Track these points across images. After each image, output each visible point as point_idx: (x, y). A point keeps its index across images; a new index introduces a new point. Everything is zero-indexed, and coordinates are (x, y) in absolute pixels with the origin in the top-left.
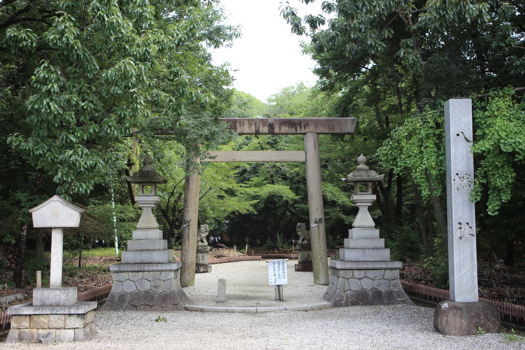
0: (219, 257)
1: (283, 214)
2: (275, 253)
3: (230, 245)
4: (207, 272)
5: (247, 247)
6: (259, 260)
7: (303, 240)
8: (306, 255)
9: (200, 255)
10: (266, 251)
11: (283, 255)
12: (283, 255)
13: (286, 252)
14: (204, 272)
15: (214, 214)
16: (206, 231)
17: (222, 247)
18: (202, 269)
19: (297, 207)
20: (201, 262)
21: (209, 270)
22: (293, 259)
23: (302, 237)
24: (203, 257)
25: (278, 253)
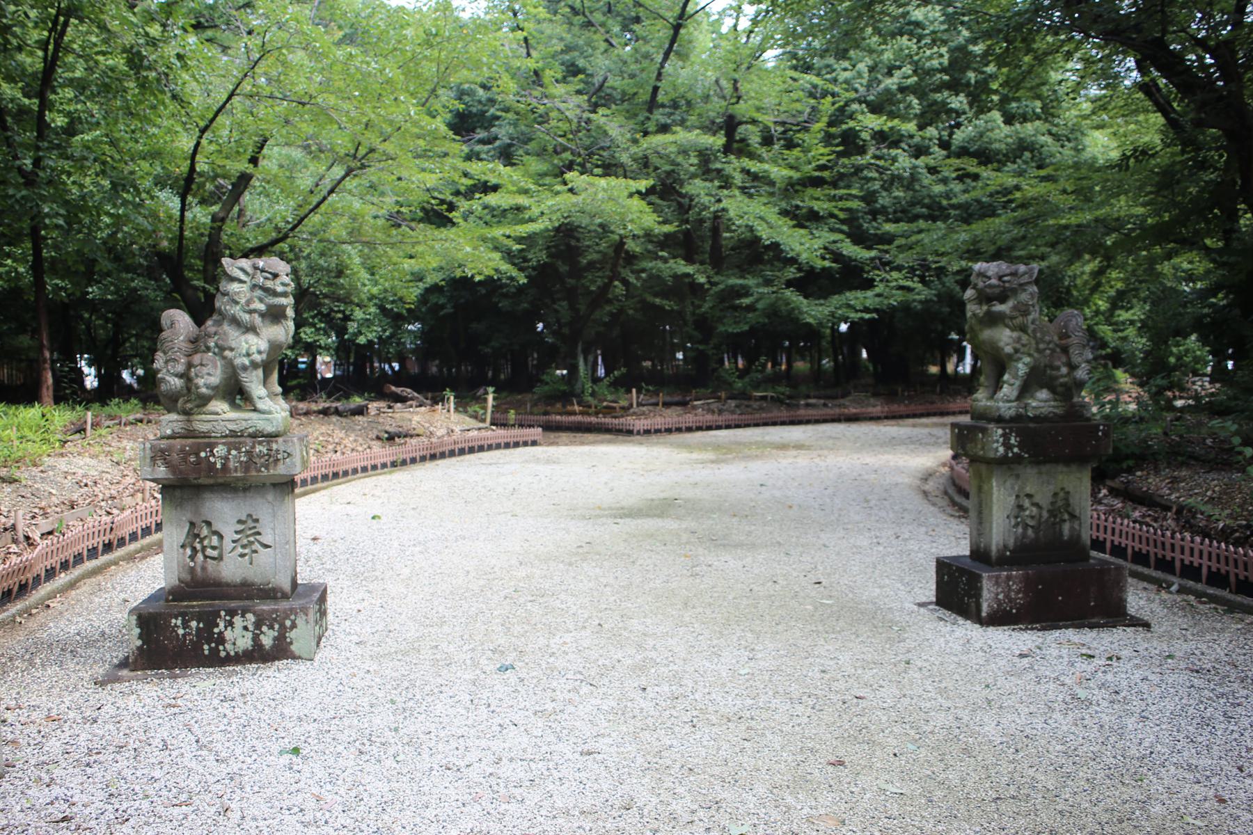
0: (391, 438)
1: (607, 287)
2: (574, 413)
3: (430, 388)
4: (281, 651)
5: (490, 397)
6: (534, 443)
7: (1025, 390)
8: (1044, 498)
9: (225, 513)
10: (541, 408)
11: (602, 419)
12: (602, 419)
13: (609, 411)
14: (257, 655)
15: (376, 283)
16: (275, 315)
17: (402, 400)
18: (238, 636)
19: (643, 270)
20: (232, 568)
21: (300, 637)
22: (638, 433)
23: (1022, 368)
24: (249, 527)
25: (582, 413)
